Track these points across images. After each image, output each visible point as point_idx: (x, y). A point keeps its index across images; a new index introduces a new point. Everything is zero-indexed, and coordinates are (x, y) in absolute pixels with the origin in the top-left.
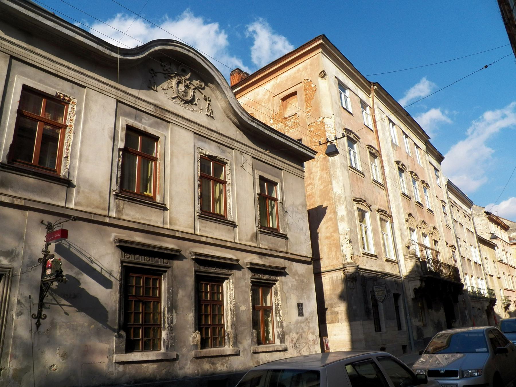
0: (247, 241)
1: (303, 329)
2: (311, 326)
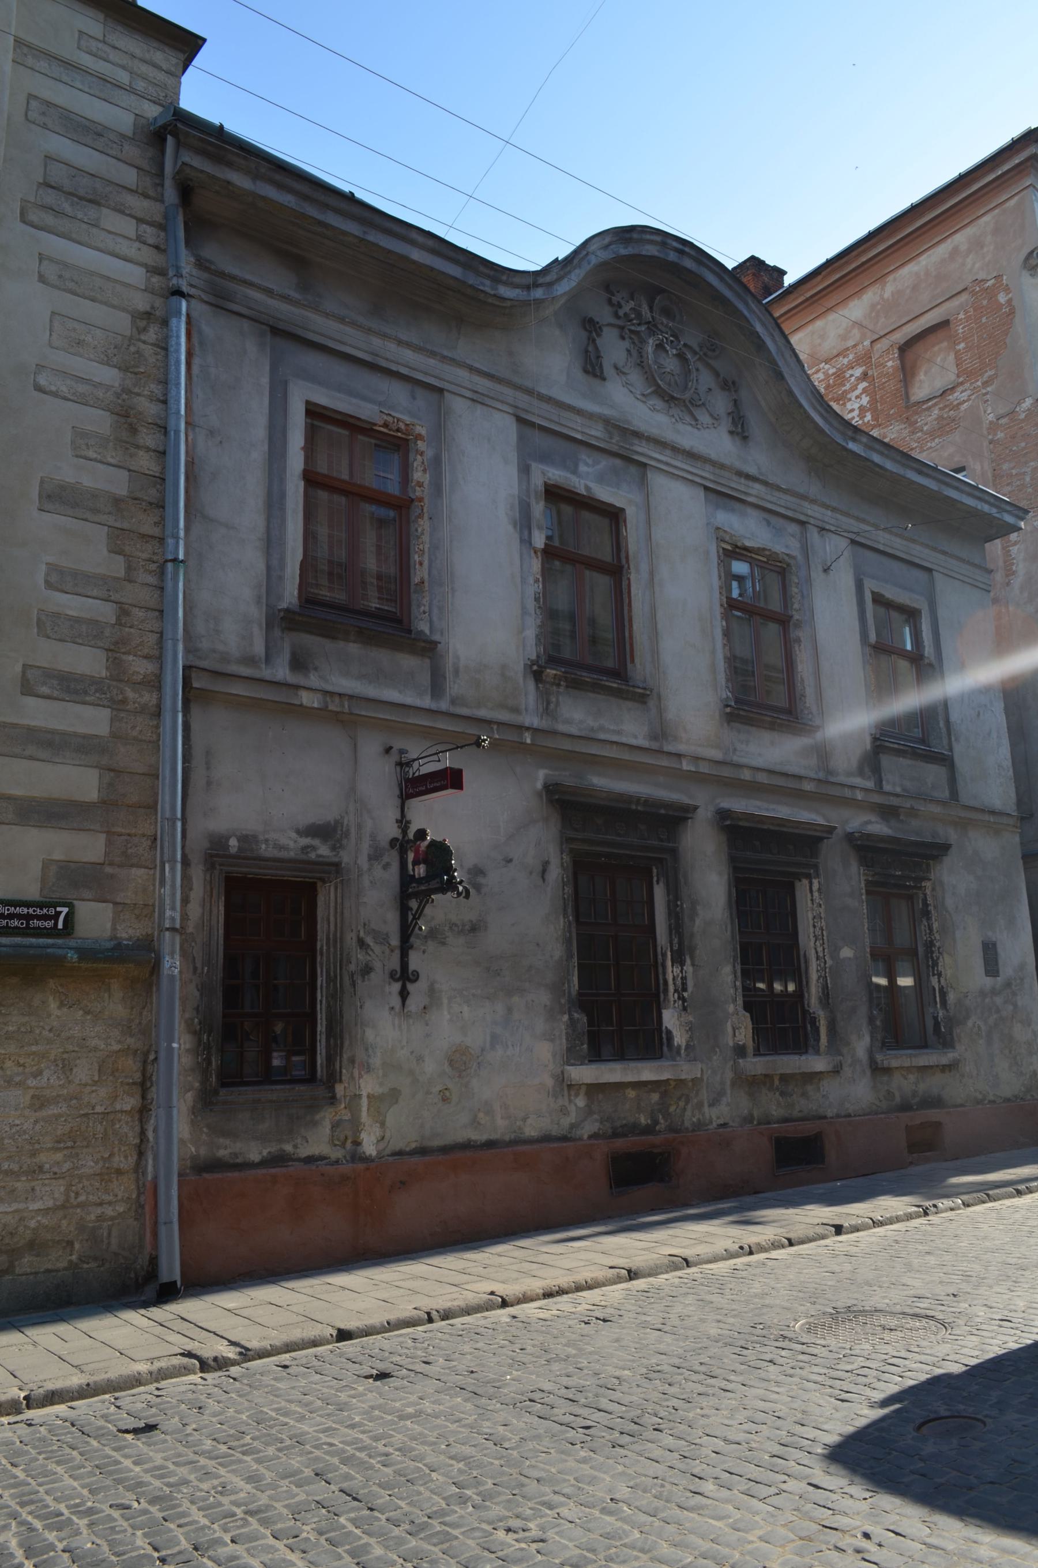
0: (849, 774)
2: (1020, 1004)
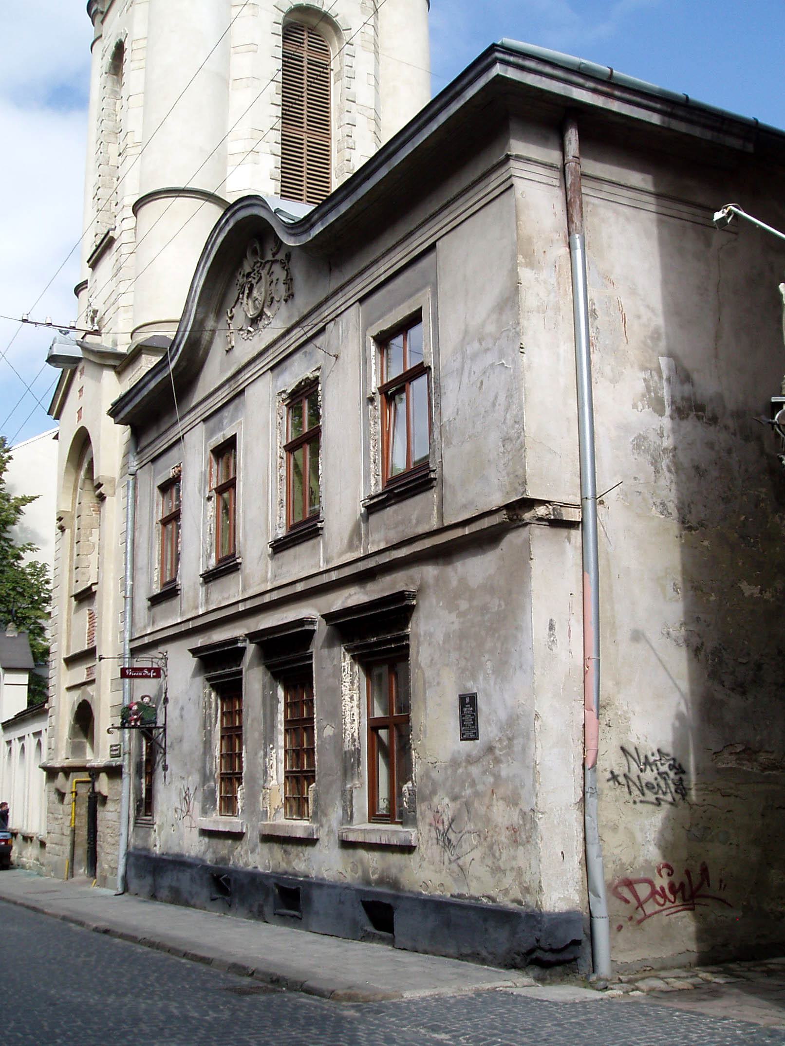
1: (473, 784)
2: (504, 773)
